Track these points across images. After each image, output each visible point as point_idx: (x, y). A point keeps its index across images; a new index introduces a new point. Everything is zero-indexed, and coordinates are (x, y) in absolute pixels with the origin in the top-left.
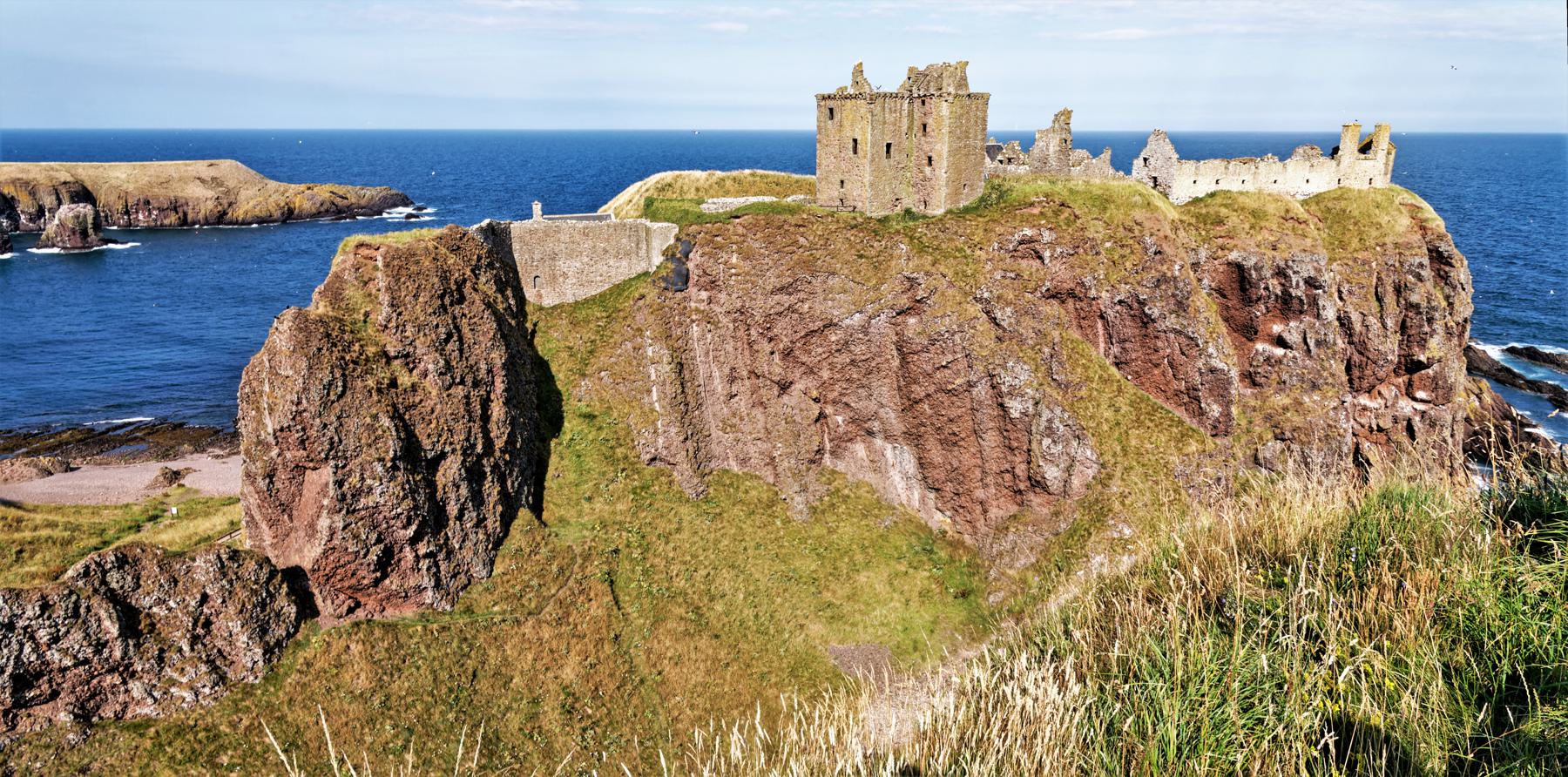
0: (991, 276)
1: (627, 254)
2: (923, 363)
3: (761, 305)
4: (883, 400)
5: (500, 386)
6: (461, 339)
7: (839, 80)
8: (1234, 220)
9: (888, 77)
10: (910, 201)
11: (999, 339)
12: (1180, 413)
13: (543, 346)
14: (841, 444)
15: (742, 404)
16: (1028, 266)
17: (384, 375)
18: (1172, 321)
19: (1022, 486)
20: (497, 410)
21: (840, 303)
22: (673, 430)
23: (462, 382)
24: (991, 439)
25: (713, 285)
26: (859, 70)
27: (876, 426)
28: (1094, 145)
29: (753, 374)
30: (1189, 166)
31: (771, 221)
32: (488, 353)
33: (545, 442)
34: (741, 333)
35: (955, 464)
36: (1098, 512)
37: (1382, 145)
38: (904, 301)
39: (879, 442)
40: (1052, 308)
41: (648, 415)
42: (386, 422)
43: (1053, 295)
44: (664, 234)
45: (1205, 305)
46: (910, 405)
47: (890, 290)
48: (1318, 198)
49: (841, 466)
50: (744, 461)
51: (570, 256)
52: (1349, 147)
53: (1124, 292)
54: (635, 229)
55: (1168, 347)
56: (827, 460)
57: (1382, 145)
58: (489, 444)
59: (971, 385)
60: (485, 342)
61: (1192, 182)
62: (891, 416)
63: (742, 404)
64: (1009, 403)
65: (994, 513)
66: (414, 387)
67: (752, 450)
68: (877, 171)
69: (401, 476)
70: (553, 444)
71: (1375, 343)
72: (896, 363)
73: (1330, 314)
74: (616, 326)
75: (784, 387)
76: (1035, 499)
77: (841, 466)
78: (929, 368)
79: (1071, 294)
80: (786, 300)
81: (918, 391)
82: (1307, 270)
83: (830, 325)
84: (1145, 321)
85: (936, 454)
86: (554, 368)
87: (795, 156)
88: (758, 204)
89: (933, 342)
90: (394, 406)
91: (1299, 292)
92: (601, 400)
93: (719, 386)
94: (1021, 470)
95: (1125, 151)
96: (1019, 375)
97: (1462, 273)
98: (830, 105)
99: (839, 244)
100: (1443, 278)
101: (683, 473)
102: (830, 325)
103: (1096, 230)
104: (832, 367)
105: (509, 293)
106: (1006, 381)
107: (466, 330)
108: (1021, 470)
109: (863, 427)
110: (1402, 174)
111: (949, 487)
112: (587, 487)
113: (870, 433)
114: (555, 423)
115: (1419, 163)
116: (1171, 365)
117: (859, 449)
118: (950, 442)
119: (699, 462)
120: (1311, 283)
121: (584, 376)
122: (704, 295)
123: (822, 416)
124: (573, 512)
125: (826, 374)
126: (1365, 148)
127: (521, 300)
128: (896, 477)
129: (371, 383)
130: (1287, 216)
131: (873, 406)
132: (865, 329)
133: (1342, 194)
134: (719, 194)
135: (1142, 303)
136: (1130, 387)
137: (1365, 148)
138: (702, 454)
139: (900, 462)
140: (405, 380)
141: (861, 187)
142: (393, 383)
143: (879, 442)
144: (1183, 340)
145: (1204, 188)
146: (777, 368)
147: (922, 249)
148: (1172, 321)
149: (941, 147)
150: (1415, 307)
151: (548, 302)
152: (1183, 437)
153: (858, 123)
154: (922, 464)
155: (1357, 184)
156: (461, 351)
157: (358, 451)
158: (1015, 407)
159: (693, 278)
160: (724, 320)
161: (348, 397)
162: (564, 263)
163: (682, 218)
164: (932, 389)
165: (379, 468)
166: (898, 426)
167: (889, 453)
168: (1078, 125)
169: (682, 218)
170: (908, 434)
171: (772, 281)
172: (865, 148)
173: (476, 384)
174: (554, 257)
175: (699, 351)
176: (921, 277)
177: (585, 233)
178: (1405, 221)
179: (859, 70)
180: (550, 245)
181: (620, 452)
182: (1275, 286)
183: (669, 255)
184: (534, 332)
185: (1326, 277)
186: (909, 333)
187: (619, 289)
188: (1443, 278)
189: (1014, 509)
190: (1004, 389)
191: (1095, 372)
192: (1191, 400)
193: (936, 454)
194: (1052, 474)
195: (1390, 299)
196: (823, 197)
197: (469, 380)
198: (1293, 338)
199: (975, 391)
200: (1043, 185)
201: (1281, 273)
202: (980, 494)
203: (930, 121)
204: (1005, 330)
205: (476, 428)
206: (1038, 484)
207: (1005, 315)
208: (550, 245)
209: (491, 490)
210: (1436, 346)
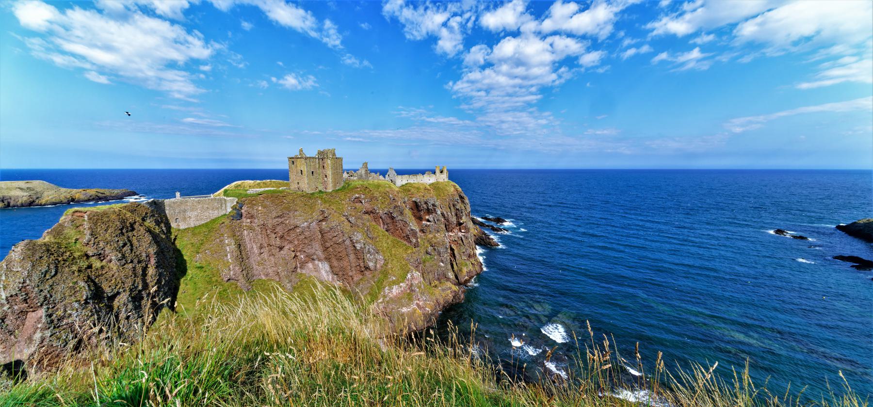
0: (347, 209)
1: (217, 209)
2: (328, 236)
3: (270, 223)
4: (317, 249)
5: (153, 261)
6: (132, 245)
7: (295, 153)
8: (413, 190)
9: (311, 151)
10: (320, 188)
12: (405, 242)
13: (179, 244)
14: (303, 264)
15: (265, 256)
16: (358, 205)
17: (84, 264)
18: (400, 218)
20: (151, 271)
21: (301, 220)
22: (237, 268)
23: (132, 262)
24: (352, 257)
25: (252, 217)
26: (301, 151)
27: (315, 257)
28: (375, 171)
29: (269, 245)
30: (400, 177)
31: (274, 197)
32: (146, 247)
33: (178, 280)
34: (264, 232)
36: (385, 274)
37: (445, 171)
38: (321, 218)
39: (316, 262)
40: (366, 217)
41: (226, 265)
42: (82, 284)
43: (366, 213)
44: (231, 202)
45: (408, 213)
46: (326, 249)
47: (316, 215)
48: (432, 184)
49: (304, 272)
50: (267, 275)
51: (192, 210)
52: (438, 171)
53: (386, 211)
54: (221, 200)
55: (400, 225)
56: (299, 270)
57: (445, 171)
58: (146, 286)
59: (344, 241)
60: (145, 245)
61: (401, 181)
62: (320, 253)
63: (265, 256)
64: (356, 245)
65: (355, 279)
66: (102, 268)
67: (270, 271)
68: (309, 179)
69: (90, 307)
70: (182, 280)
71: (450, 219)
72: (320, 237)
73: (439, 213)
74: (213, 234)
75: (281, 248)
76: (367, 273)
77: (304, 272)
79: (371, 212)
80: (280, 220)
81: (328, 245)
82: (432, 202)
83: (296, 227)
84: (393, 218)
85: (335, 263)
86: (183, 253)
87: (283, 175)
88: (270, 191)
89: (331, 229)
90: (89, 277)
92: (206, 261)
93: (256, 250)
94: (362, 264)
95: (384, 173)
96: (358, 237)
97: (467, 201)
98: (293, 160)
99: (298, 202)
100: (463, 202)
101: (242, 282)
102: (296, 227)
103: (377, 194)
104: (298, 240)
105: (162, 225)
106: (355, 238)
107: (135, 241)
108: (362, 264)
109: (310, 258)
110: (451, 177)
111: (341, 273)
112: (198, 295)
113: (313, 259)
114: (184, 272)
115: (453, 175)
117: (310, 265)
118: (340, 259)
119: (249, 278)
120: (433, 205)
121: (198, 253)
122: (249, 220)
123: (296, 256)
124: (191, 305)
125: (296, 243)
126: (442, 172)
127: (169, 227)
128: (323, 272)
129: (75, 268)
130: (425, 189)
131: (313, 251)
132: (308, 227)
133: (438, 183)
134: (251, 187)
136: (391, 237)
137: (442, 172)
138: (249, 275)
139: (324, 268)
140: (97, 264)
141: (305, 185)
142: (90, 267)
143: (316, 262)
145: (404, 182)
146: (278, 242)
147: (325, 202)
148: (400, 218)
149: (329, 172)
150: (457, 209)
151: (182, 227)
152: (407, 249)
153: (302, 166)
154: (331, 267)
155: (441, 180)
156: (132, 250)
157: (63, 299)
158: (358, 246)
159: (244, 215)
160: (257, 228)
161: (59, 275)
162: (187, 215)
163: (238, 196)
165: (76, 305)
166: (322, 256)
167: (320, 265)
168: (370, 167)
169: (238, 196)
170: (326, 258)
171: (274, 214)
172: (305, 172)
173: (139, 262)
174: (185, 211)
175: (247, 239)
176: (325, 210)
177: (199, 202)
178: (452, 189)
179: (301, 151)
180: (183, 207)
181: (214, 279)
182: (425, 206)
183: (234, 208)
184: (175, 239)
185: (437, 204)
186: (323, 227)
187: (214, 221)
188: (463, 202)
189: (361, 277)
191: (381, 234)
192: (407, 238)
193: (335, 263)
194: (371, 264)
195: (452, 208)
196: (292, 188)
197: (136, 261)
198: (431, 219)
200: (361, 182)
201: (426, 203)
202: (350, 274)
205: (139, 280)
206: (367, 268)
207: (352, 219)
208: (183, 207)
209: (146, 304)
210: (464, 219)
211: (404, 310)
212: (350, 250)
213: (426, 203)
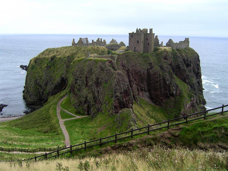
19: (169, 95)
35: (157, 93)
39: (143, 92)
73: (192, 66)
91: (189, 63)
135: (179, 65)
144: (184, 71)
154: (150, 94)
158: (168, 82)
164: (154, 81)
166: (146, 89)
194: (174, 92)
202: (161, 98)
203: (148, 38)
213: (187, 60)
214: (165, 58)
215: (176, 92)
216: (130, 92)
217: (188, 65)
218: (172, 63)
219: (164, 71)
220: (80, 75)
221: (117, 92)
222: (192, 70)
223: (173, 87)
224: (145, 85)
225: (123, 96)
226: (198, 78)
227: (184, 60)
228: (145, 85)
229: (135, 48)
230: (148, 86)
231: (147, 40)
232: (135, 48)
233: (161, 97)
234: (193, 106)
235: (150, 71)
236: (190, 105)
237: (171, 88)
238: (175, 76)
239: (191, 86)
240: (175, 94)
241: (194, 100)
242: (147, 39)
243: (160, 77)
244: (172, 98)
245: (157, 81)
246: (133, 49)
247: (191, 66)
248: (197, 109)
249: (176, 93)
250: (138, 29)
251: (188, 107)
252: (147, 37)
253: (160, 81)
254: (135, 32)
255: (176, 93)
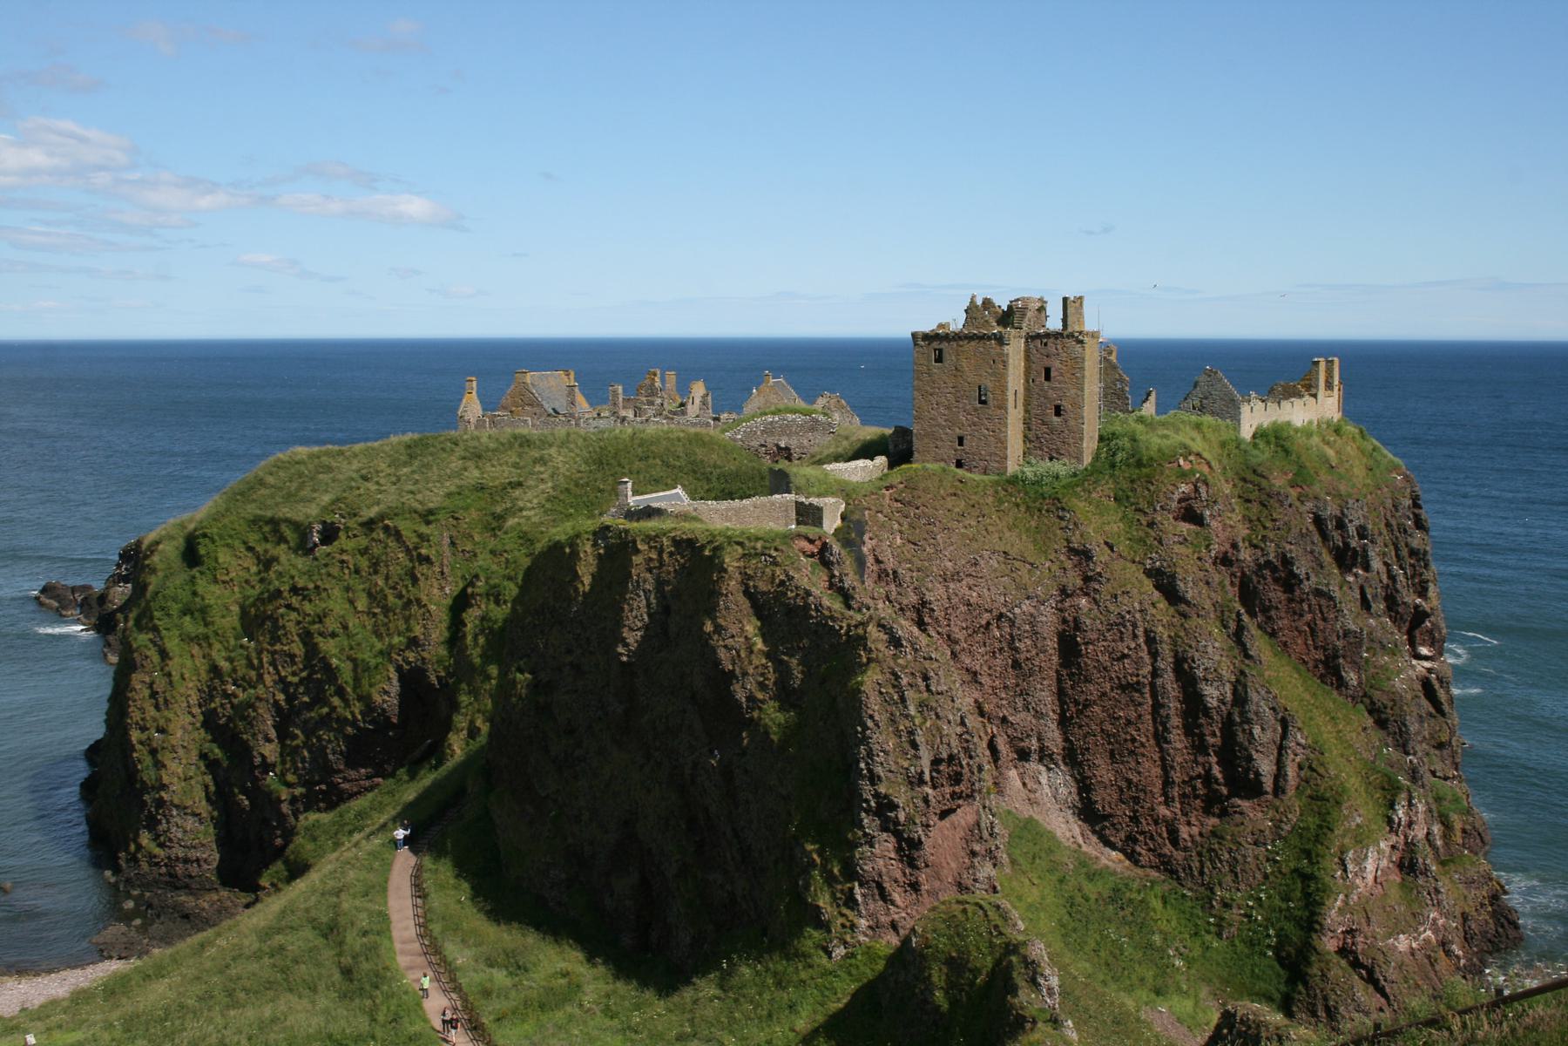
2: (1095, 652)
11: (1184, 616)
24: (1178, 740)
35: (1134, 778)
73: (1376, 564)
78: (1104, 659)
81: (1092, 691)
84: (1289, 582)
91: (1353, 544)
116: (1313, 631)
135: (1287, 562)
150: (1413, 553)
154: (1084, 786)
190: (1200, 673)
199: (1159, 681)
202: (1163, 811)
203: (1056, 364)
204: (1188, 603)
211: (1403, 943)
212: (1173, 705)
213: (1341, 525)
214: (1191, 515)
215: (1280, 764)
216: (980, 769)
217: (1347, 558)
218: (1234, 546)
219: (1183, 607)
220: (569, 652)
221: (879, 770)
222: (1375, 596)
223: (1257, 731)
224: (1039, 715)
225: (926, 800)
226: (1426, 658)
227: (1318, 521)
228: (1039, 715)
229: (961, 441)
230: (1064, 722)
231: (1048, 378)
232: (961, 441)
233: (1168, 802)
234: (1408, 865)
235: (1078, 608)
236: (1384, 863)
237: (1241, 737)
238: (1259, 644)
239: (1373, 710)
240: (1268, 784)
241: (1410, 824)
242: (1048, 371)
243: (1154, 655)
244: (1245, 804)
245: (1136, 687)
246: (949, 450)
247: (1367, 567)
248: (1437, 891)
249: (1280, 775)
250: (979, 303)
251: (1370, 878)
252: (1047, 362)
253: (1153, 685)
254: (956, 321)
255: (1280, 775)
